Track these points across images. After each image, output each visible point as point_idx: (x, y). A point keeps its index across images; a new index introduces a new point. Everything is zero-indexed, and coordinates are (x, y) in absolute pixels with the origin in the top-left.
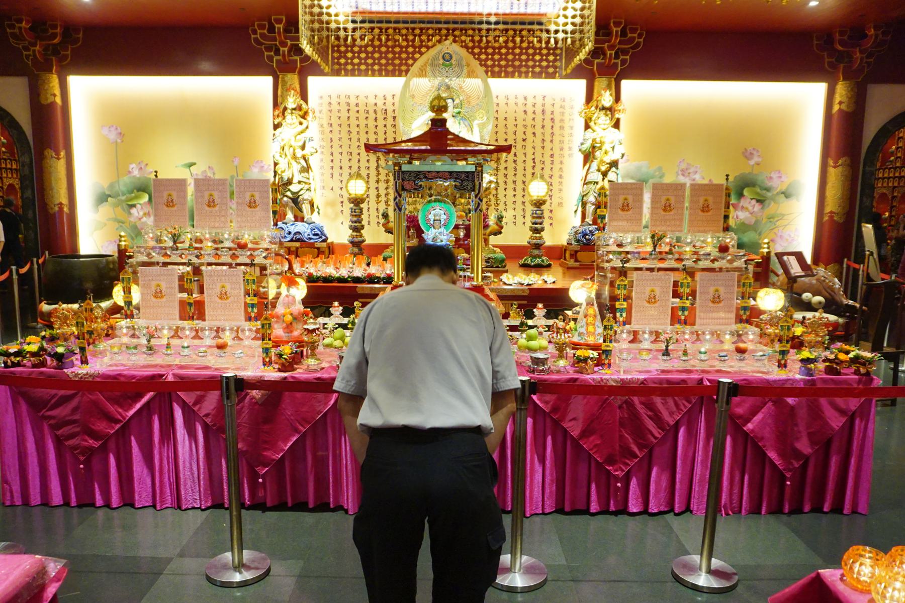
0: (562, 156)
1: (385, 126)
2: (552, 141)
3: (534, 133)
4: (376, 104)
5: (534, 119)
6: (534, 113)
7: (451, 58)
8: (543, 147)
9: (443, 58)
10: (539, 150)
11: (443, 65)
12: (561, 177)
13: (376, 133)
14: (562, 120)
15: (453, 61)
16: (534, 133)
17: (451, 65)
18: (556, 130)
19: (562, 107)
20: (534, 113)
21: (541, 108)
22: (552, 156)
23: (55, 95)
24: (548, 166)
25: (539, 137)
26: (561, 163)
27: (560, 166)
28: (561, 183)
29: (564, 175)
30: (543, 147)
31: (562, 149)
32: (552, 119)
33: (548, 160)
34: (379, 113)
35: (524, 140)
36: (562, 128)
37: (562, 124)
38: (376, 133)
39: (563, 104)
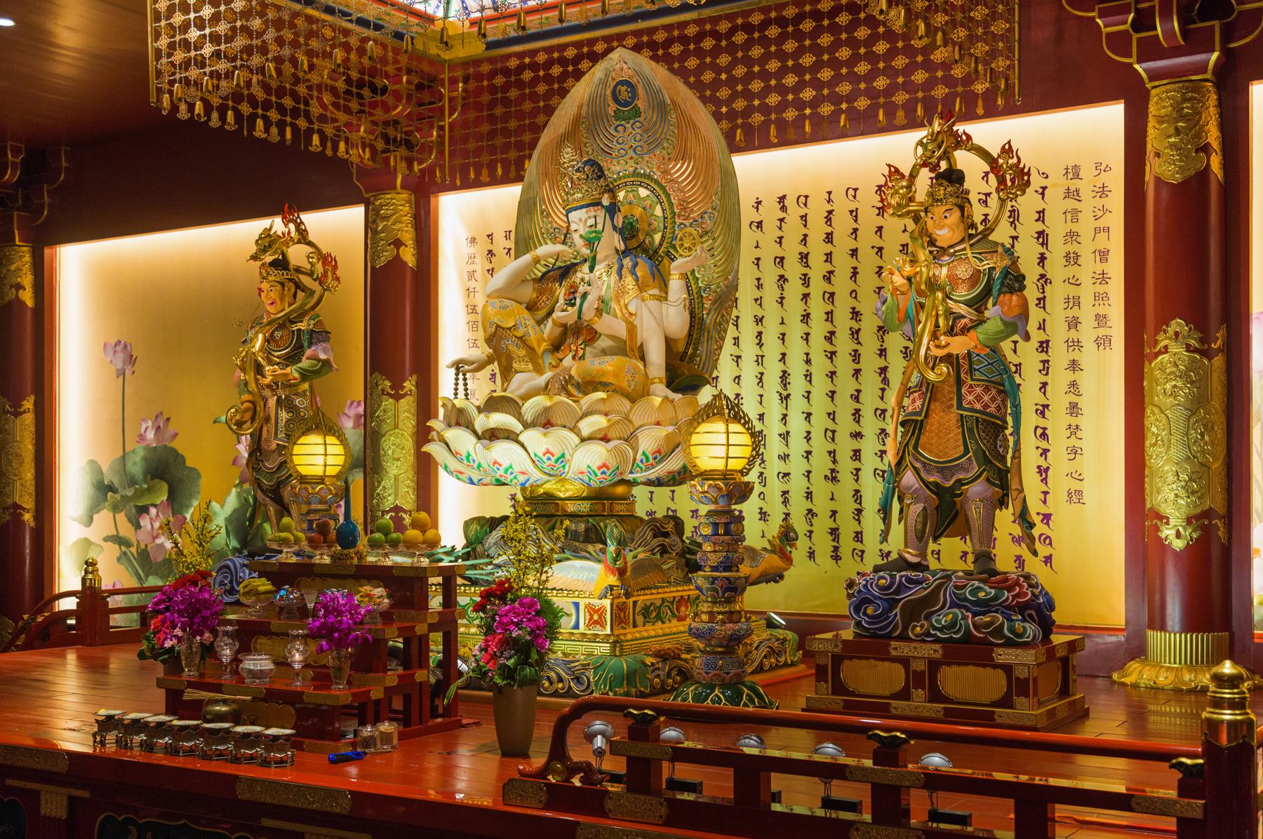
0: (1075, 344)
2: (1041, 301)
7: (634, 95)
12: (1074, 409)
14: (1072, 236)
19: (1068, 194)
23: (19, 287)
26: (1074, 365)
27: (1070, 376)
28: (1074, 430)
29: (1083, 403)
31: (1074, 324)
36: (1072, 259)
39: (1074, 185)
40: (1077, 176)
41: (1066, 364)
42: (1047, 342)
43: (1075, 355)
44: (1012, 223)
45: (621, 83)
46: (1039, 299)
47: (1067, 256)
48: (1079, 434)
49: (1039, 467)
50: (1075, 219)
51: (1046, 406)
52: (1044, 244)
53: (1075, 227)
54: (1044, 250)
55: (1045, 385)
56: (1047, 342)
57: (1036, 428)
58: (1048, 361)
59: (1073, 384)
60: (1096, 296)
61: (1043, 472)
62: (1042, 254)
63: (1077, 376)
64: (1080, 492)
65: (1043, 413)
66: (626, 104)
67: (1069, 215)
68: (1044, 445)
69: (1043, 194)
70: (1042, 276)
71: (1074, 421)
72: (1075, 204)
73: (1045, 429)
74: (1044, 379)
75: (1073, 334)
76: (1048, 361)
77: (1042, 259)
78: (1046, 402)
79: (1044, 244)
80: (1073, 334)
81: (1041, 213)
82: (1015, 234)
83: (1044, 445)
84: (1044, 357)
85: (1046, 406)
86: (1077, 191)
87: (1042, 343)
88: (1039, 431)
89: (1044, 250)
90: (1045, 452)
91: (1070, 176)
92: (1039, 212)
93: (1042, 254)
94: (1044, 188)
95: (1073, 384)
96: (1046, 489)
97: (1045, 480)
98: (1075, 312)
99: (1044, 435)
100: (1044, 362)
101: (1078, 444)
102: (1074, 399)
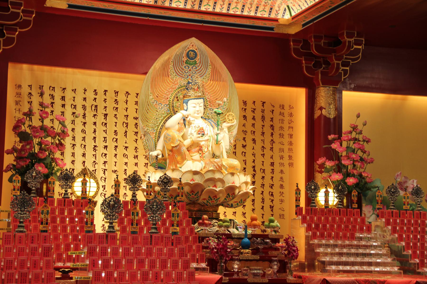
1: (95, 123)
2: (272, 149)
3: (254, 140)
4: (85, 99)
5: (253, 125)
6: (254, 118)
7: (196, 55)
8: (263, 155)
9: (188, 55)
10: (259, 159)
11: (186, 62)
12: (282, 186)
13: (83, 131)
14: (282, 128)
15: (197, 60)
16: (254, 140)
17: (196, 63)
18: (276, 138)
20: (254, 118)
21: (261, 114)
22: (272, 164)
24: (268, 175)
25: (259, 144)
26: (282, 172)
27: (280, 175)
30: (263, 155)
31: (282, 157)
32: (272, 126)
33: (268, 169)
34: (88, 109)
35: (244, 146)
36: (281, 136)
37: (282, 132)
38: (83, 131)
39: (282, 111)
40: (283, 108)
41: (279, 171)
42: (273, 163)
43: (282, 168)
44: (263, 120)
45: (193, 51)
46: (271, 148)
47: (280, 134)
48: (283, 195)
49: (270, 206)
50: (283, 123)
51: (273, 185)
52: (273, 129)
53: (282, 125)
54: (273, 131)
55: (272, 177)
56: (273, 163)
57: (270, 192)
58: (273, 169)
59: (281, 178)
60: (289, 149)
61: (272, 207)
62: (272, 133)
63: (283, 175)
64: (283, 215)
65: (272, 187)
66: (192, 59)
67: (281, 121)
68: (272, 198)
69: (273, 112)
70: (272, 140)
71: (282, 190)
72: (282, 118)
73: (272, 193)
74: (272, 175)
75: (281, 161)
76: (273, 169)
77: (272, 134)
78: (273, 183)
79: (273, 129)
80: (281, 161)
81: (272, 119)
82: (263, 124)
83: (272, 198)
84: (272, 168)
85: (273, 185)
86: (283, 113)
87: (272, 163)
88: (271, 193)
89: (273, 131)
90: (272, 200)
91: (281, 108)
92: (271, 118)
93: (272, 133)
94: (273, 110)
95: (281, 178)
96: (272, 213)
97: (272, 211)
98: (282, 154)
99: (272, 195)
100: (273, 170)
101: (283, 198)
102: (282, 183)
